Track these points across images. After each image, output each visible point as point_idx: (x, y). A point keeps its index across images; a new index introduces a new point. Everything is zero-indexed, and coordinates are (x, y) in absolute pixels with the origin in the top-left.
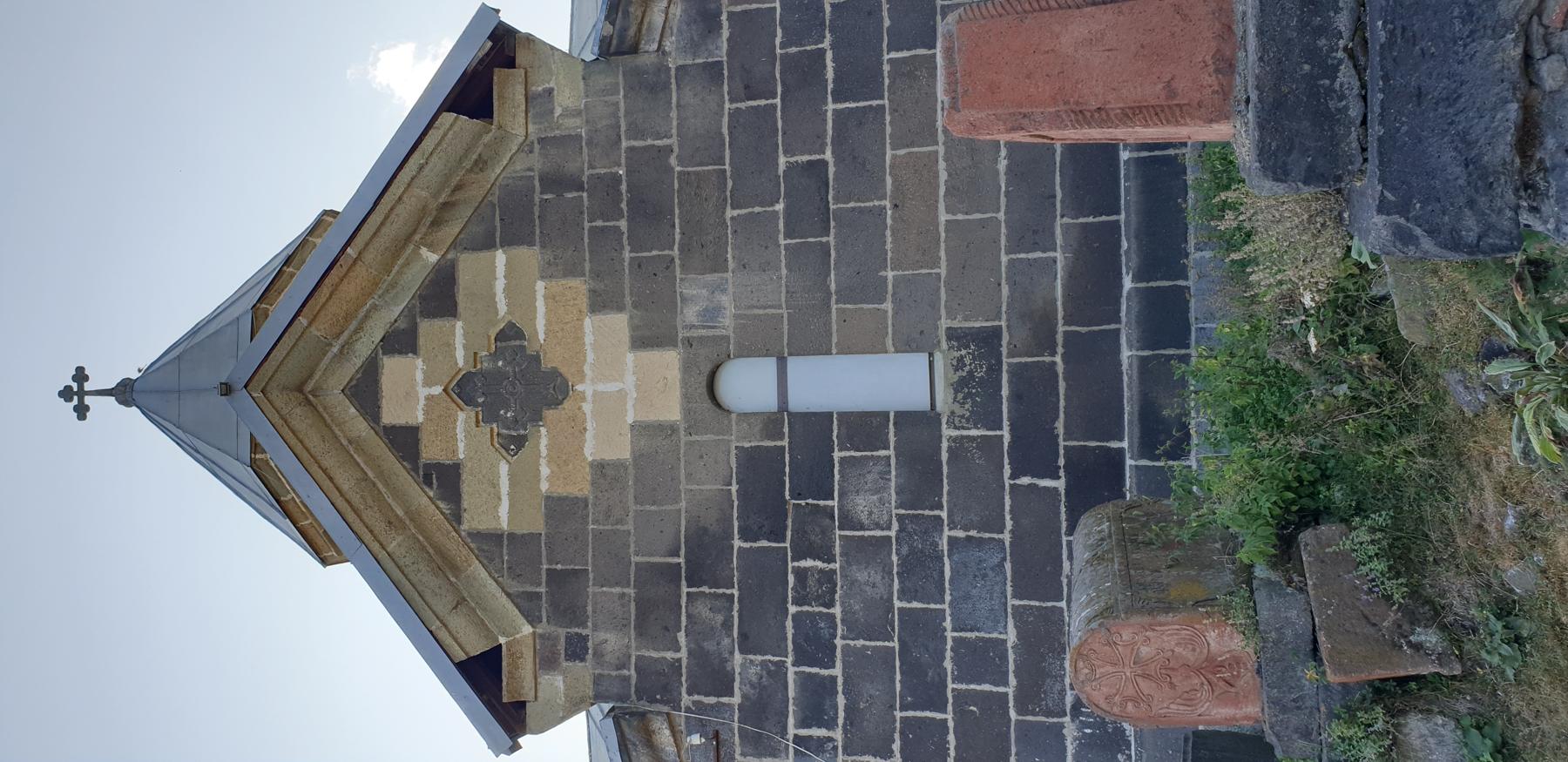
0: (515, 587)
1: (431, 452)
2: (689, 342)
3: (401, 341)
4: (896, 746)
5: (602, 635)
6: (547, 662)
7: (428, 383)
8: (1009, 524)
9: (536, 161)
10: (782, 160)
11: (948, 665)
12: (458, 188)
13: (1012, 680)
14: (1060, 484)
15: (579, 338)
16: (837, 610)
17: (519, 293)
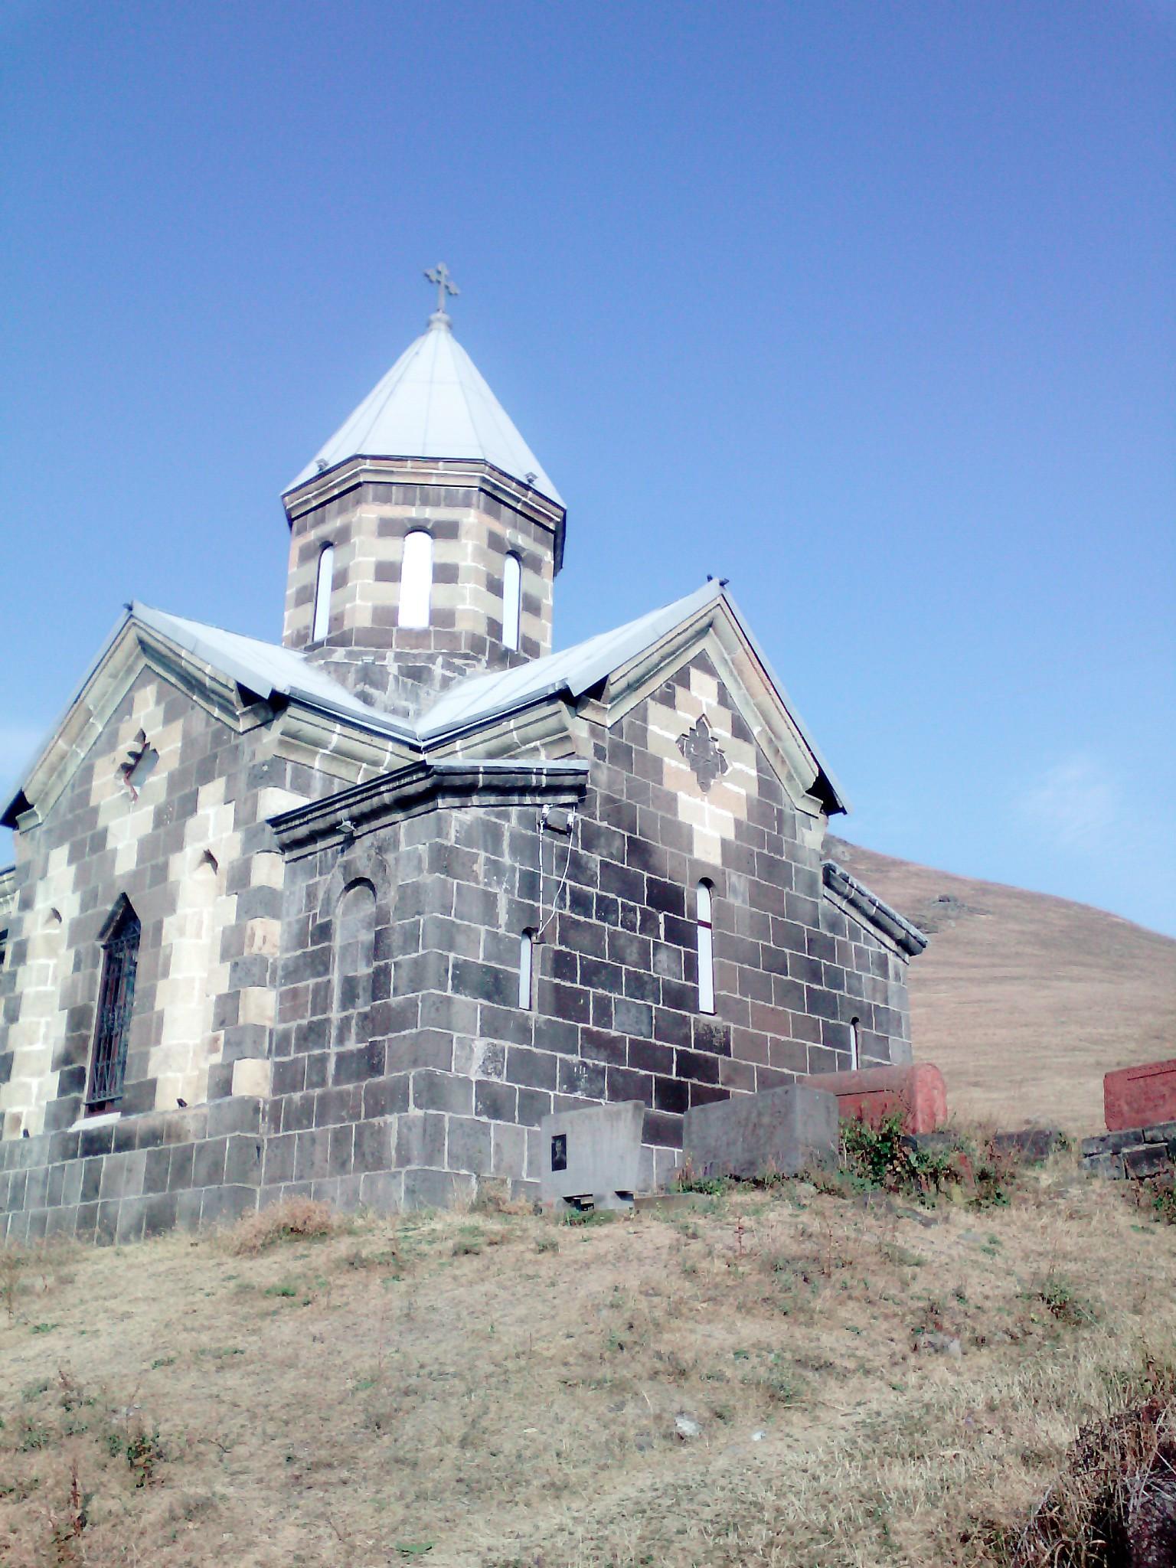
0: (625, 722)
1: (679, 690)
2: (724, 873)
3: (723, 698)
4: (563, 948)
5: (605, 771)
6: (595, 729)
7: (708, 706)
8: (659, 1043)
9: (787, 811)
10: (787, 951)
11: (600, 991)
12: (783, 762)
13: (596, 1029)
14: (674, 1077)
15: (724, 806)
16: (619, 929)
17: (739, 778)
